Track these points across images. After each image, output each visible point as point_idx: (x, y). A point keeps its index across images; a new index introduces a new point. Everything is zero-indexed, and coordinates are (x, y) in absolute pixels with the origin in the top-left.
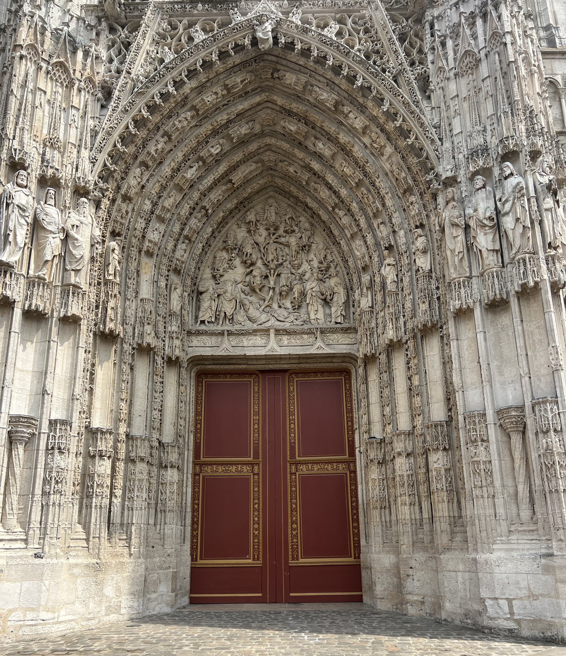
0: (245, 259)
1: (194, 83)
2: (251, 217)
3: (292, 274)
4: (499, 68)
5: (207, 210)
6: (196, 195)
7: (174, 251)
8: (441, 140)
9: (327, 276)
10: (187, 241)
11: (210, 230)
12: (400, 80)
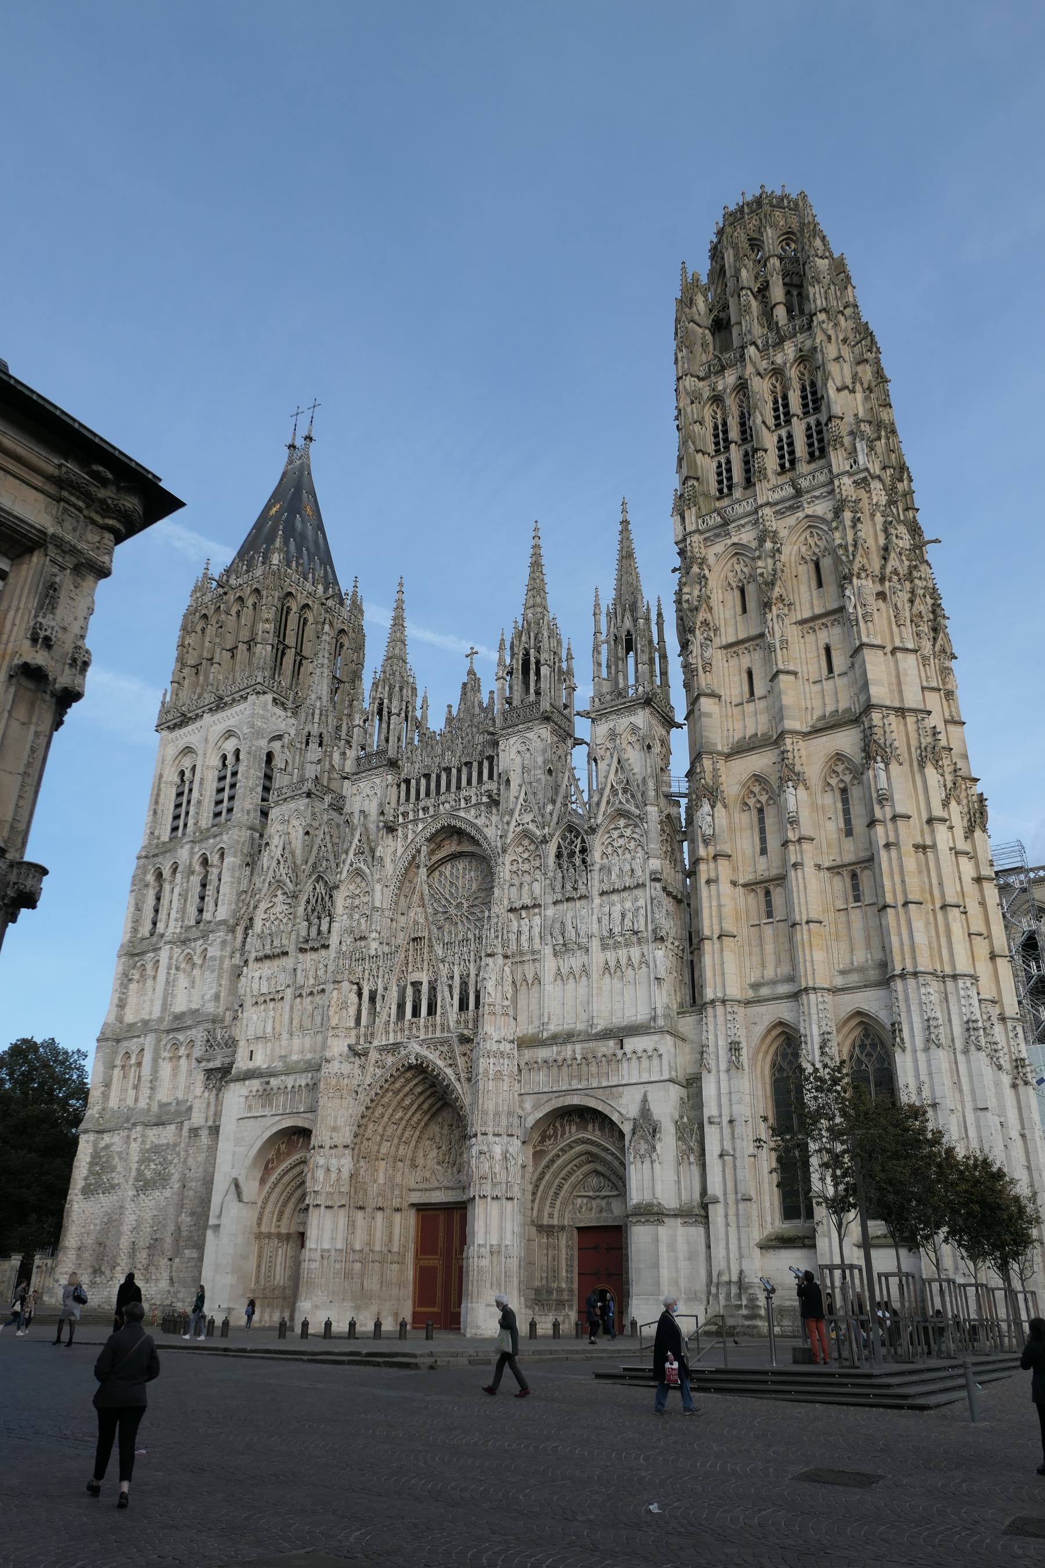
2: (440, 1120)
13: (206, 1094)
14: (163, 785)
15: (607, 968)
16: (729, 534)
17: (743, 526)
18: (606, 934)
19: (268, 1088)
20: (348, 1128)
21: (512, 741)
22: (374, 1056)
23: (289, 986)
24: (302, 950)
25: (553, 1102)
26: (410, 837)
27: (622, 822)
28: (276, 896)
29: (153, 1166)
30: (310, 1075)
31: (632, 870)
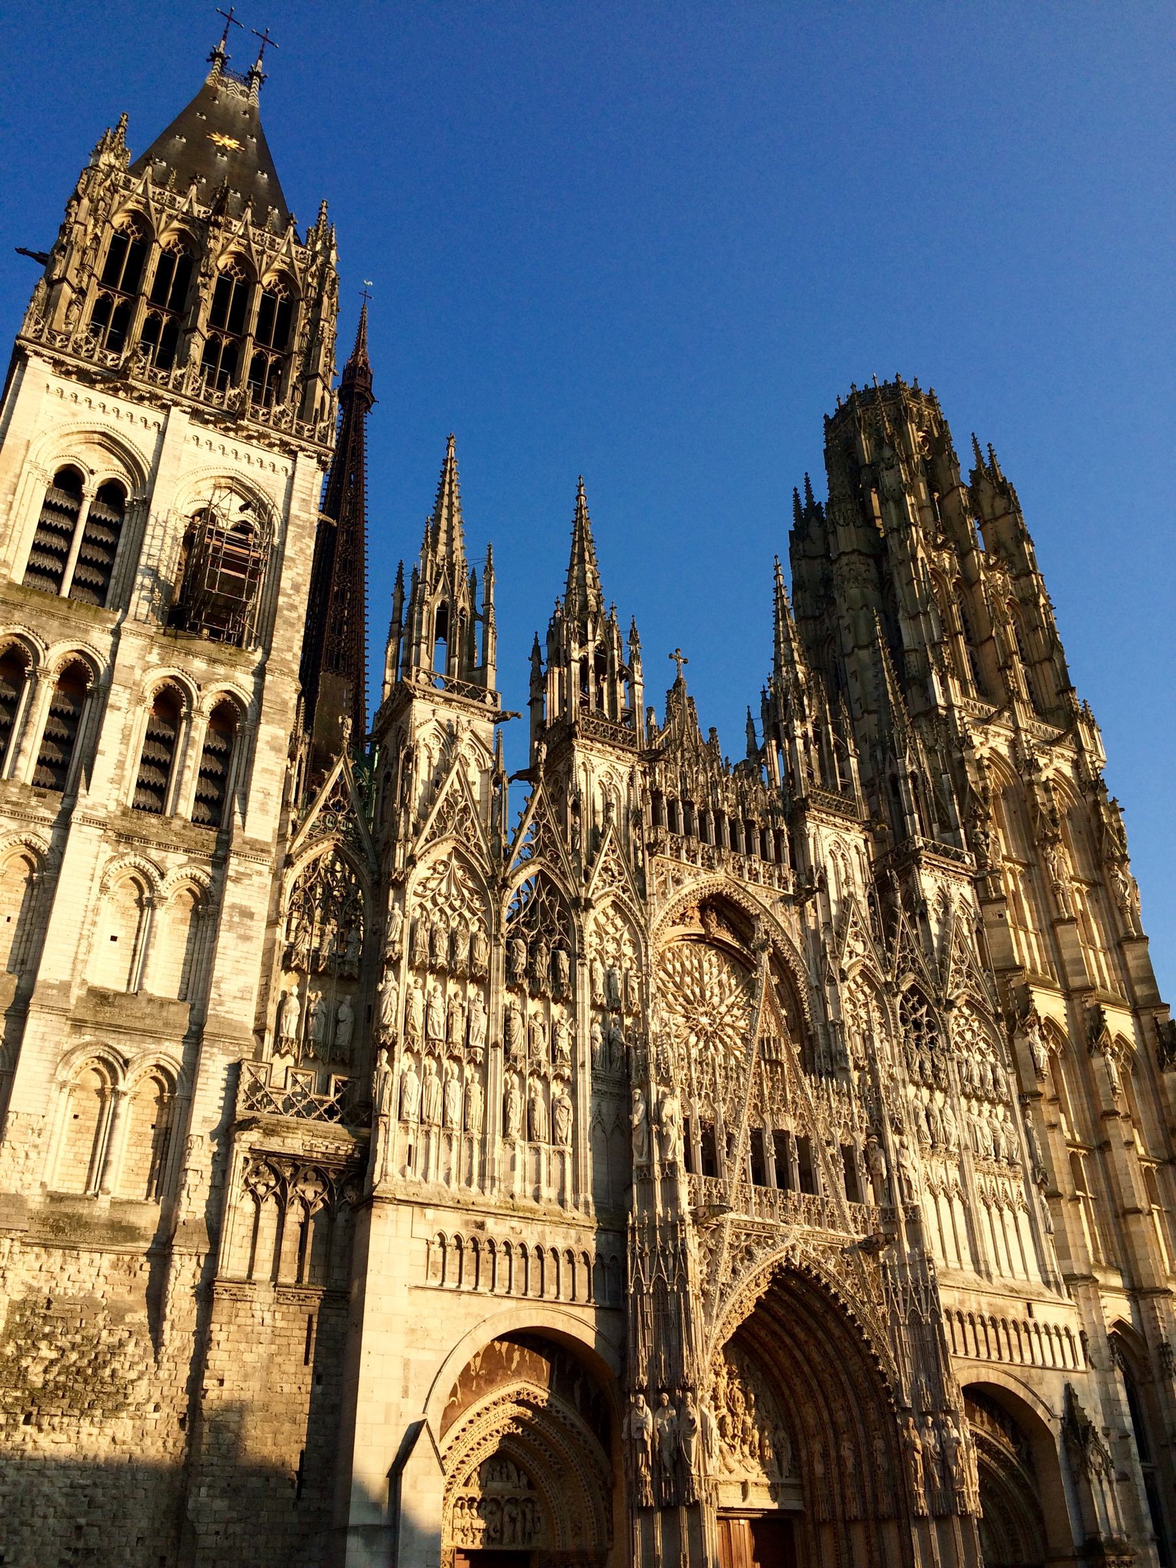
13: (248, 1205)
14: (27, 467)
16: (986, 734)
17: (999, 735)
19: (482, 1237)
21: (825, 831)
22: (727, 1234)
23: (496, 1045)
27: (966, 1012)
29: (46, 1352)
30: (573, 1232)
31: (996, 1082)
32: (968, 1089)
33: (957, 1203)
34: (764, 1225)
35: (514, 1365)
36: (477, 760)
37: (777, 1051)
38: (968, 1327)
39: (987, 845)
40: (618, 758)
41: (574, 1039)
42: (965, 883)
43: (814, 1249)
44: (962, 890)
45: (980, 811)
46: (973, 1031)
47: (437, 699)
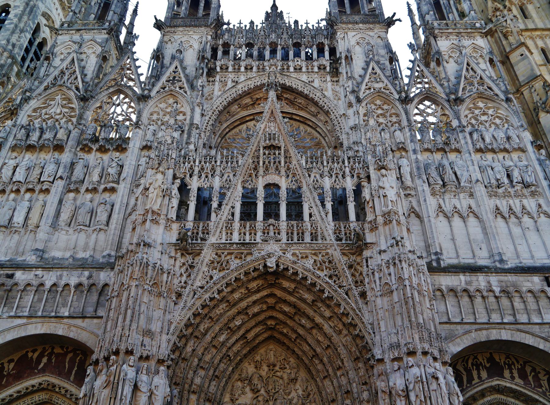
0: (253, 388)
1: (229, 289)
2: (258, 358)
3: (284, 398)
4: (403, 299)
5: (230, 358)
6: (224, 350)
7: (209, 387)
8: (374, 333)
9: (308, 401)
10: (216, 379)
11: (231, 368)
12: (349, 293)
15: (498, 211)
18: (493, 181)
20: (164, 337)
21: (351, 34)
22: (208, 254)
23: (61, 178)
24: (86, 149)
25: (473, 335)
26: (230, 84)
27: (481, 105)
28: (54, 99)
30: (86, 273)
31: (508, 138)
32: (480, 145)
33: (472, 221)
34: (243, 244)
35: (42, 365)
36: (94, 53)
37: (270, 139)
38: (479, 300)
39: (506, 21)
40: (194, 32)
41: (122, 167)
42: (478, 38)
43: (294, 254)
44: (475, 42)
45: (499, 6)
46: (487, 114)
47: (71, 32)
